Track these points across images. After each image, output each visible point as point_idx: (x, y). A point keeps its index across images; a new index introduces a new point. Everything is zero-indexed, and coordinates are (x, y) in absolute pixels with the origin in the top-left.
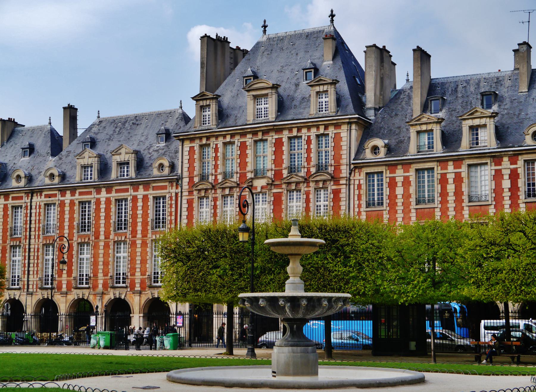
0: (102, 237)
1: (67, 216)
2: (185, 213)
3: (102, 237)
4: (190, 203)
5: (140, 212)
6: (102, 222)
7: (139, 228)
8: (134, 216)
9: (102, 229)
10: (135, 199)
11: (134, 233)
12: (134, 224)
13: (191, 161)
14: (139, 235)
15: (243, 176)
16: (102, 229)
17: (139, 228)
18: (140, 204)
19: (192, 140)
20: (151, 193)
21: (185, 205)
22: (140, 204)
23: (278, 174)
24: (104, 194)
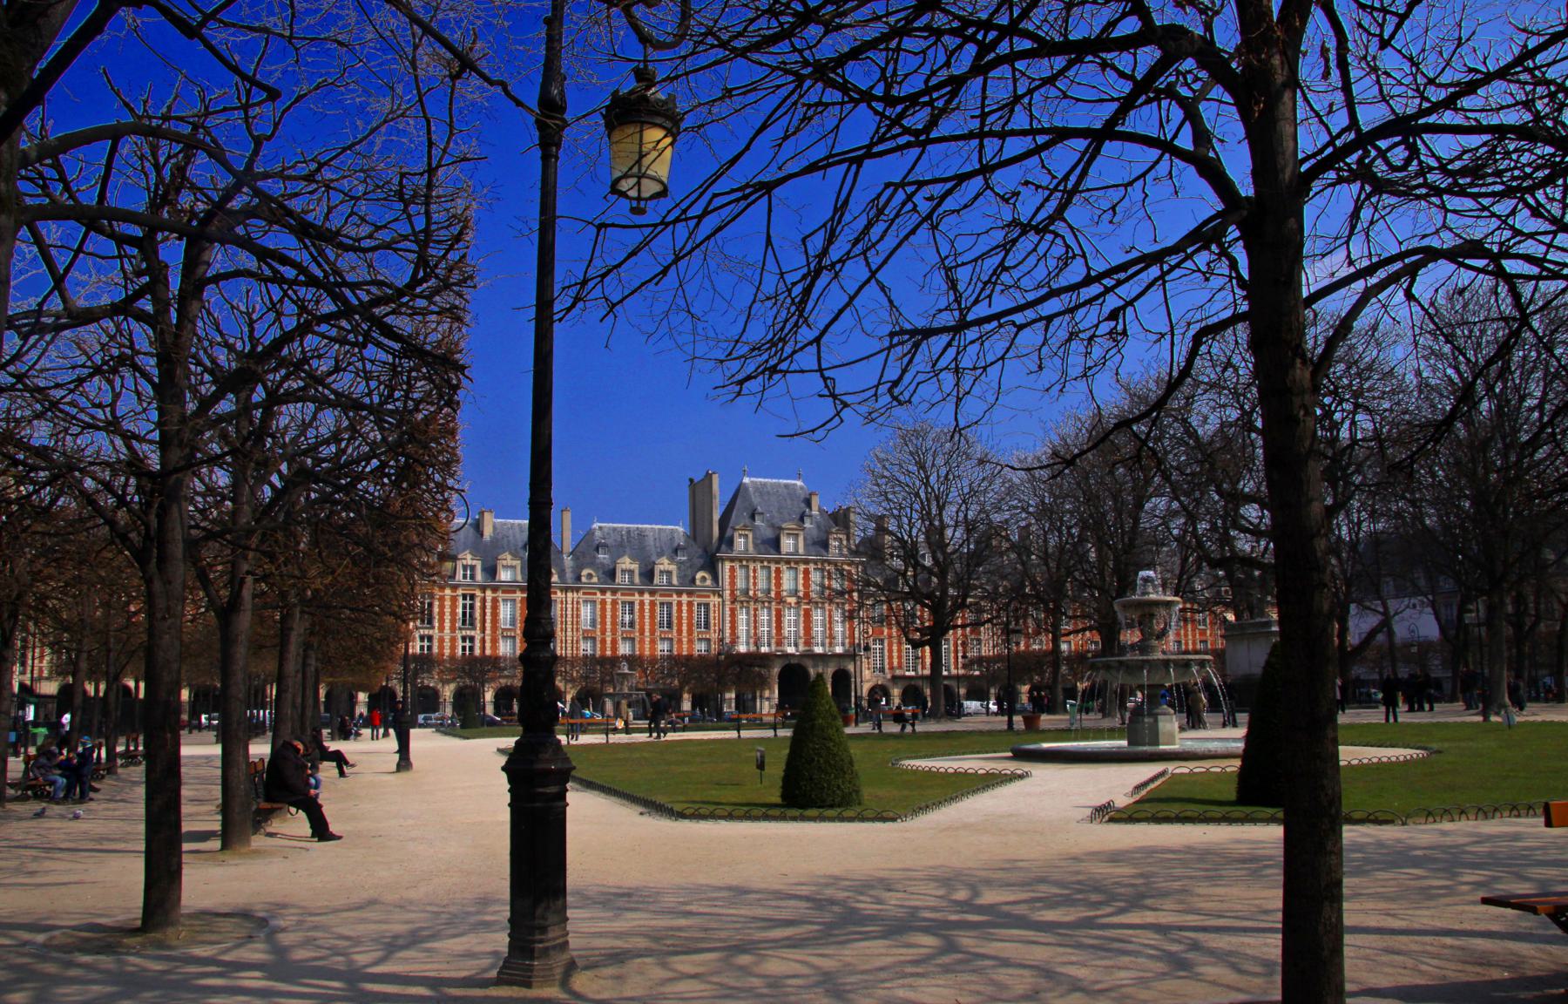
0: (647, 633)
1: (609, 614)
2: (728, 619)
3: (647, 633)
4: (733, 611)
5: (685, 615)
6: (647, 620)
7: (685, 628)
8: (680, 618)
9: (647, 627)
10: (680, 604)
11: (680, 631)
12: (680, 624)
13: (733, 577)
14: (685, 633)
15: (778, 593)
16: (647, 627)
17: (685, 628)
18: (685, 608)
19: (732, 560)
20: (696, 600)
21: (728, 612)
22: (685, 608)
23: (807, 595)
24: (647, 597)
